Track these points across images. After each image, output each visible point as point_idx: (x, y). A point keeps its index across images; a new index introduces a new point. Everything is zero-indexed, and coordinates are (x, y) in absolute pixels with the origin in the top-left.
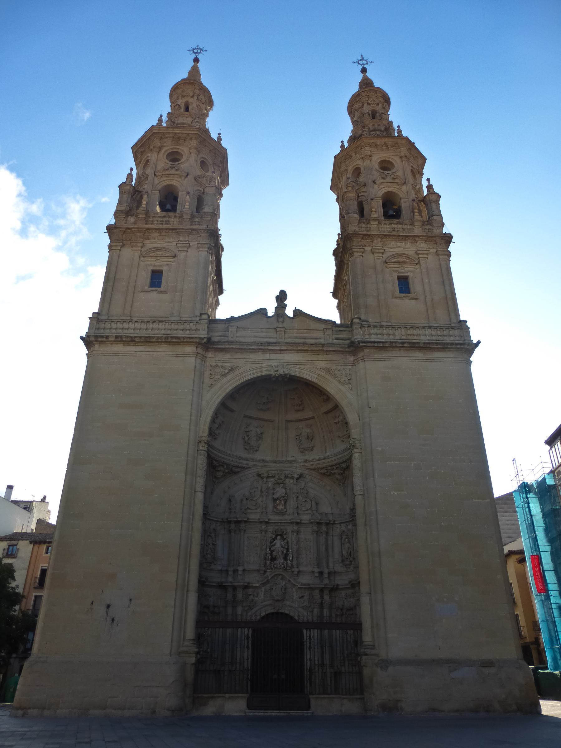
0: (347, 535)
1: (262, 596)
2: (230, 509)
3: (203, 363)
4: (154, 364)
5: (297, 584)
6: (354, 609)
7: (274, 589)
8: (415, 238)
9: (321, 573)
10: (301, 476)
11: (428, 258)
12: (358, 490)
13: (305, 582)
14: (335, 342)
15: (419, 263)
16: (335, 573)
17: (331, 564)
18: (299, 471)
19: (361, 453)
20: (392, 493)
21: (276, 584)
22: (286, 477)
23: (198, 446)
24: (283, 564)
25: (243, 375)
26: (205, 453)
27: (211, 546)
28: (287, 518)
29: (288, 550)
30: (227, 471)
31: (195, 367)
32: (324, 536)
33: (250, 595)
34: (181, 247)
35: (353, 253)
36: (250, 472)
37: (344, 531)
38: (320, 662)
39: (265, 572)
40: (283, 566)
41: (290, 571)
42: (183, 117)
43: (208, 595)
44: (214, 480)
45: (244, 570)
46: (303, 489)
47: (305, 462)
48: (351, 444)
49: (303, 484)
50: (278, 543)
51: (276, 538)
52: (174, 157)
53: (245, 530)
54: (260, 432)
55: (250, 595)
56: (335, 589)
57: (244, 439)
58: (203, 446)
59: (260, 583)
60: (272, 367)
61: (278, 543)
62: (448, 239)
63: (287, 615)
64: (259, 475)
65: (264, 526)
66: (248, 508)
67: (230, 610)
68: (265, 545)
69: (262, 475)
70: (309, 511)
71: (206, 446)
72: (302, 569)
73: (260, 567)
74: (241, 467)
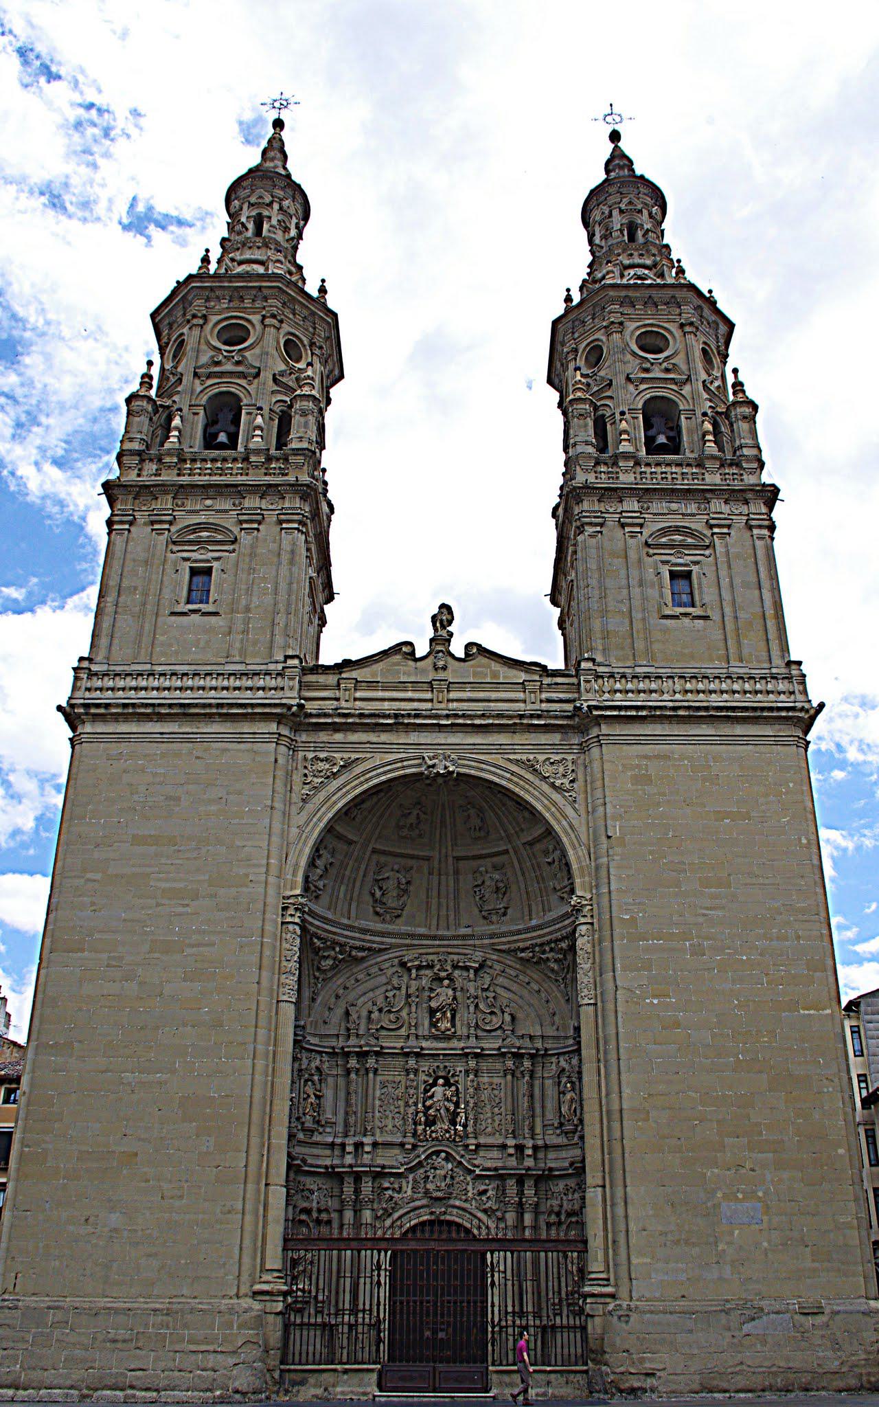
0: (569, 1077)
2: (348, 1029)
3: (291, 753)
4: (197, 758)
6: (577, 1216)
7: (431, 1178)
8: (703, 495)
9: (520, 1148)
11: (729, 534)
12: (586, 996)
13: (489, 1164)
15: (711, 546)
16: (546, 1147)
17: (538, 1130)
18: (479, 956)
19: (592, 924)
20: (648, 1001)
21: (435, 1169)
22: (455, 967)
23: (283, 915)
24: (449, 1132)
26: (297, 928)
27: (312, 1099)
29: (457, 1105)
30: (341, 957)
31: (276, 761)
32: (527, 1078)
33: (387, 1189)
34: (247, 522)
35: (582, 526)
37: (564, 1070)
38: (517, 1309)
39: (415, 1147)
40: (447, 1135)
42: (250, 248)
44: (317, 974)
45: (375, 1145)
46: (486, 990)
47: (492, 936)
48: (575, 906)
49: (487, 980)
50: (438, 1090)
51: (434, 1084)
52: (234, 335)
53: (376, 1070)
54: (404, 881)
55: (387, 1189)
56: (544, 1178)
57: (373, 895)
58: (292, 915)
60: (424, 758)
62: (771, 495)
64: (403, 964)
65: (412, 1062)
66: (382, 1027)
67: (349, 1215)
69: (409, 965)
70: (499, 1032)
71: (298, 914)
73: (405, 1137)
74: (369, 949)
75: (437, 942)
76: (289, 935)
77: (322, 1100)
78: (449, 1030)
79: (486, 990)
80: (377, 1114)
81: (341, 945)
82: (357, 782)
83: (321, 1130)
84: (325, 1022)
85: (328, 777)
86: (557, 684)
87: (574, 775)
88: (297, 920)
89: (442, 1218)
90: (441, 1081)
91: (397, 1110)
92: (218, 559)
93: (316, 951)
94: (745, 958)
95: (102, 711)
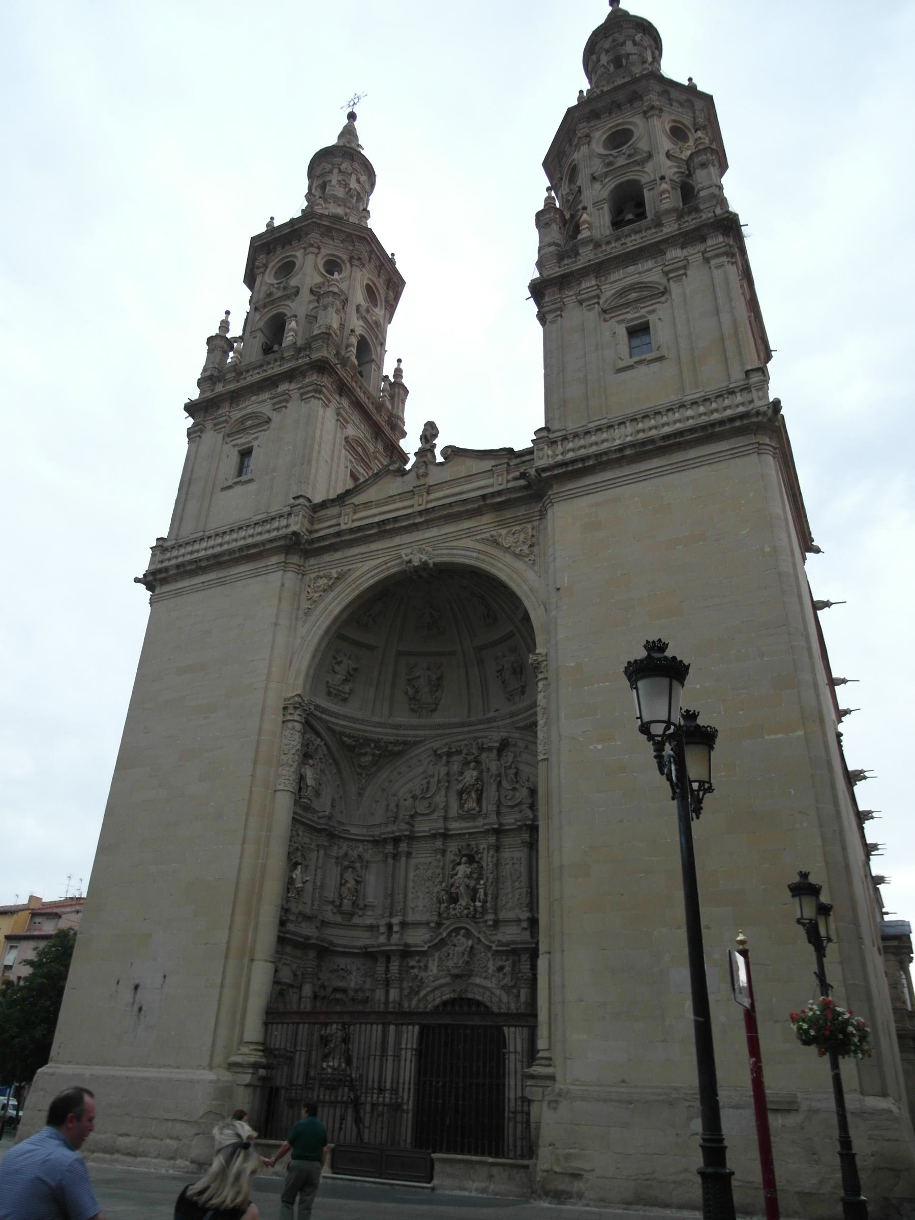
1: (434, 968)
3: (300, 576)
5: (492, 945)
7: (451, 955)
10: (504, 745)
13: (505, 938)
14: (510, 485)
21: (455, 946)
22: (482, 749)
23: (284, 715)
24: (469, 909)
25: (358, 583)
26: (298, 726)
27: (351, 884)
28: (480, 824)
30: (377, 752)
31: (283, 585)
33: (413, 967)
36: (423, 748)
39: (439, 925)
40: (465, 912)
41: (481, 920)
43: (342, 969)
44: (359, 770)
45: (404, 925)
46: (510, 767)
49: (510, 759)
50: (462, 869)
51: (459, 864)
55: (413, 967)
57: (406, 693)
58: (291, 714)
59: (429, 945)
61: (462, 869)
63: (479, 1004)
65: (439, 843)
66: (416, 813)
68: (441, 875)
69: (439, 752)
72: (503, 915)
74: (405, 743)
75: (466, 729)
76: (288, 731)
77: (362, 884)
78: (474, 809)
79: (510, 767)
80: (410, 896)
81: (376, 742)
82: (349, 589)
83: (361, 913)
84: (372, 814)
85: (325, 591)
86: (524, 462)
87: (534, 540)
88: (297, 718)
89: (464, 996)
90: (464, 859)
91: (427, 890)
92: (256, 438)
93: (351, 749)
94: (698, 686)
95: (163, 575)
